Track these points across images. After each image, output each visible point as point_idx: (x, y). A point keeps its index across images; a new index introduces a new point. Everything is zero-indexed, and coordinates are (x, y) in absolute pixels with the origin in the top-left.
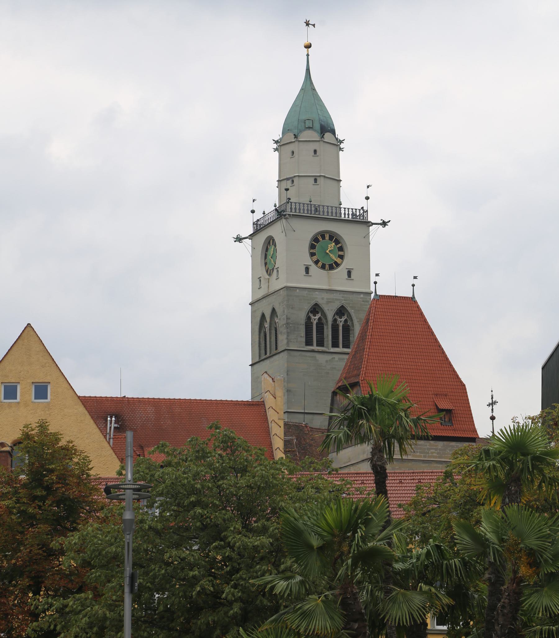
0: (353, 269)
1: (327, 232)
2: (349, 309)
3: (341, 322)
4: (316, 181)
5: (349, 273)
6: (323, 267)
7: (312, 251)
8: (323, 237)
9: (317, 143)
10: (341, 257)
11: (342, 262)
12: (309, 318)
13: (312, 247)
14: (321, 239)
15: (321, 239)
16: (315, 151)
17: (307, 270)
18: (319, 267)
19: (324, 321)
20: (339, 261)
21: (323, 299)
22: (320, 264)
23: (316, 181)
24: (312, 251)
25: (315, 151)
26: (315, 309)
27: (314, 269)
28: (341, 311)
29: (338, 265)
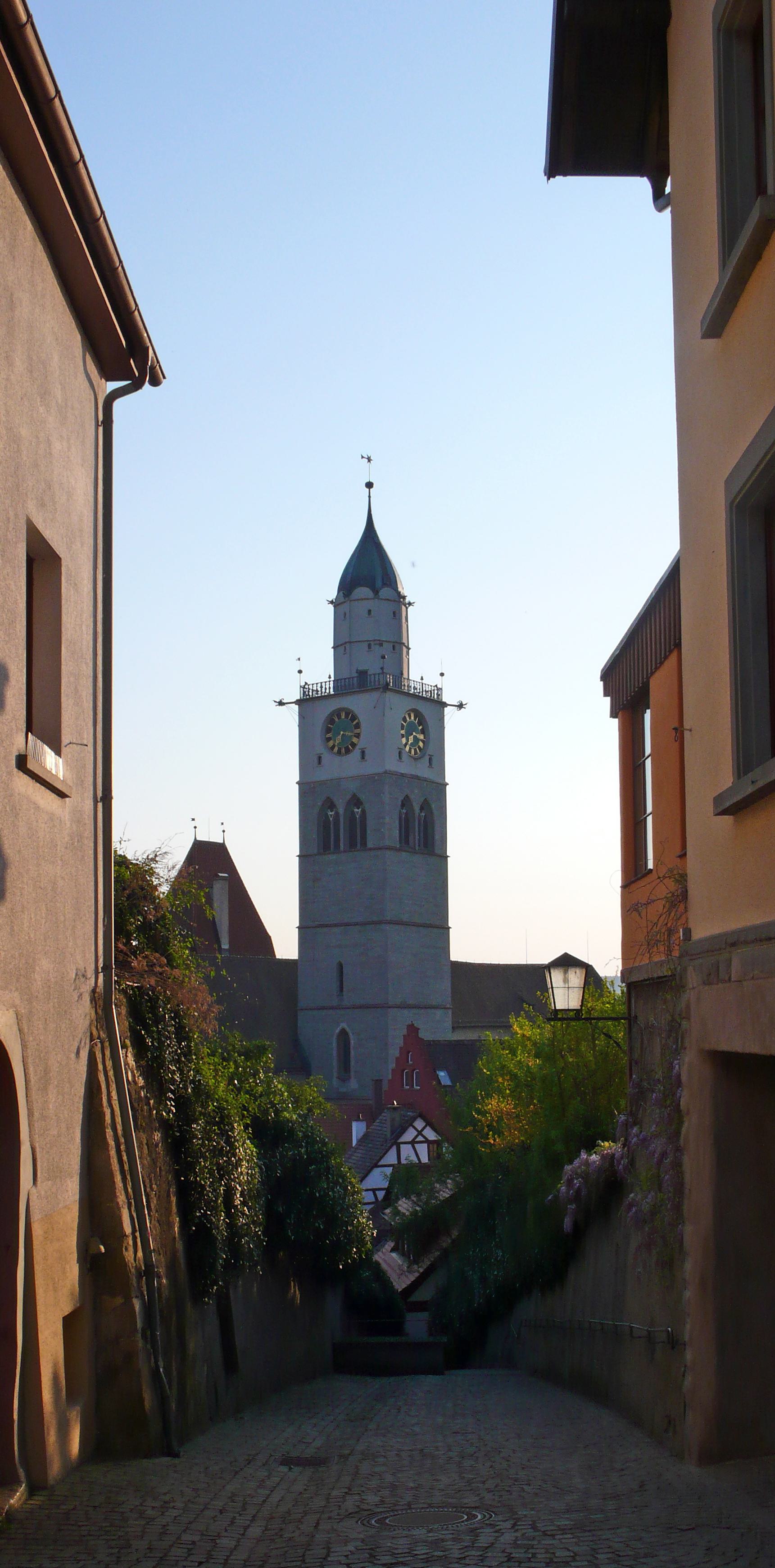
0: (365, 748)
5: (363, 753)
8: (339, 717)
10: (358, 736)
11: (358, 742)
13: (328, 730)
14: (337, 720)
15: (337, 720)
17: (320, 758)
18: (334, 753)
20: (355, 740)
24: (327, 736)
27: (327, 757)
28: (356, 801)
29: (354, 745)
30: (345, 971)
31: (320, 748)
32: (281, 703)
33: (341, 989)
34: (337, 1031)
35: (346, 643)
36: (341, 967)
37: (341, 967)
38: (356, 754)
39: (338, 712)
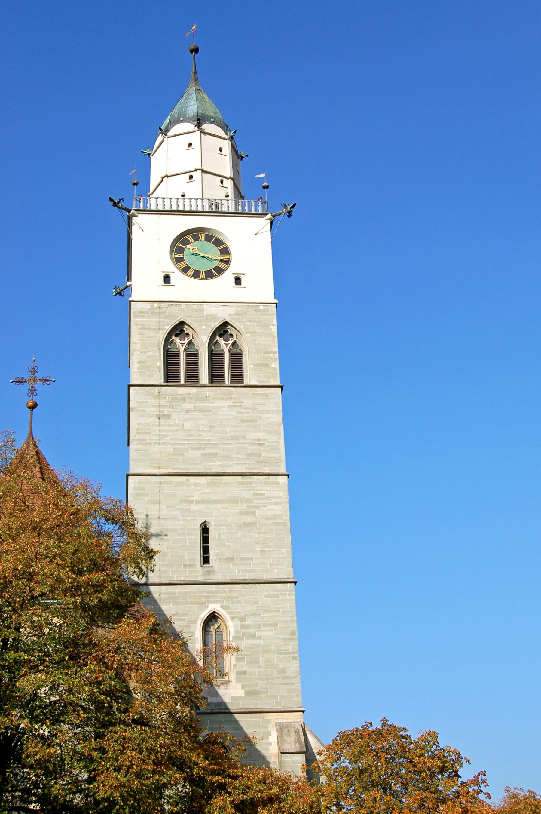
1: (201, 230)
4: (191, 177)
5: (238, 281)
7: (177, 256)
11: (227, 268)
17: (167, 279)
22: (191, 272)
23: (191, 177)
24: (177, 256)
30: (212, 534)
31: (169, 266)
32: (115, 205)
33: (206, 560)
34: (204, 614)
35: (196, 170)
36: (205, 530)
37: (205, 530)
38: (228, 277)
39: (195, 233)
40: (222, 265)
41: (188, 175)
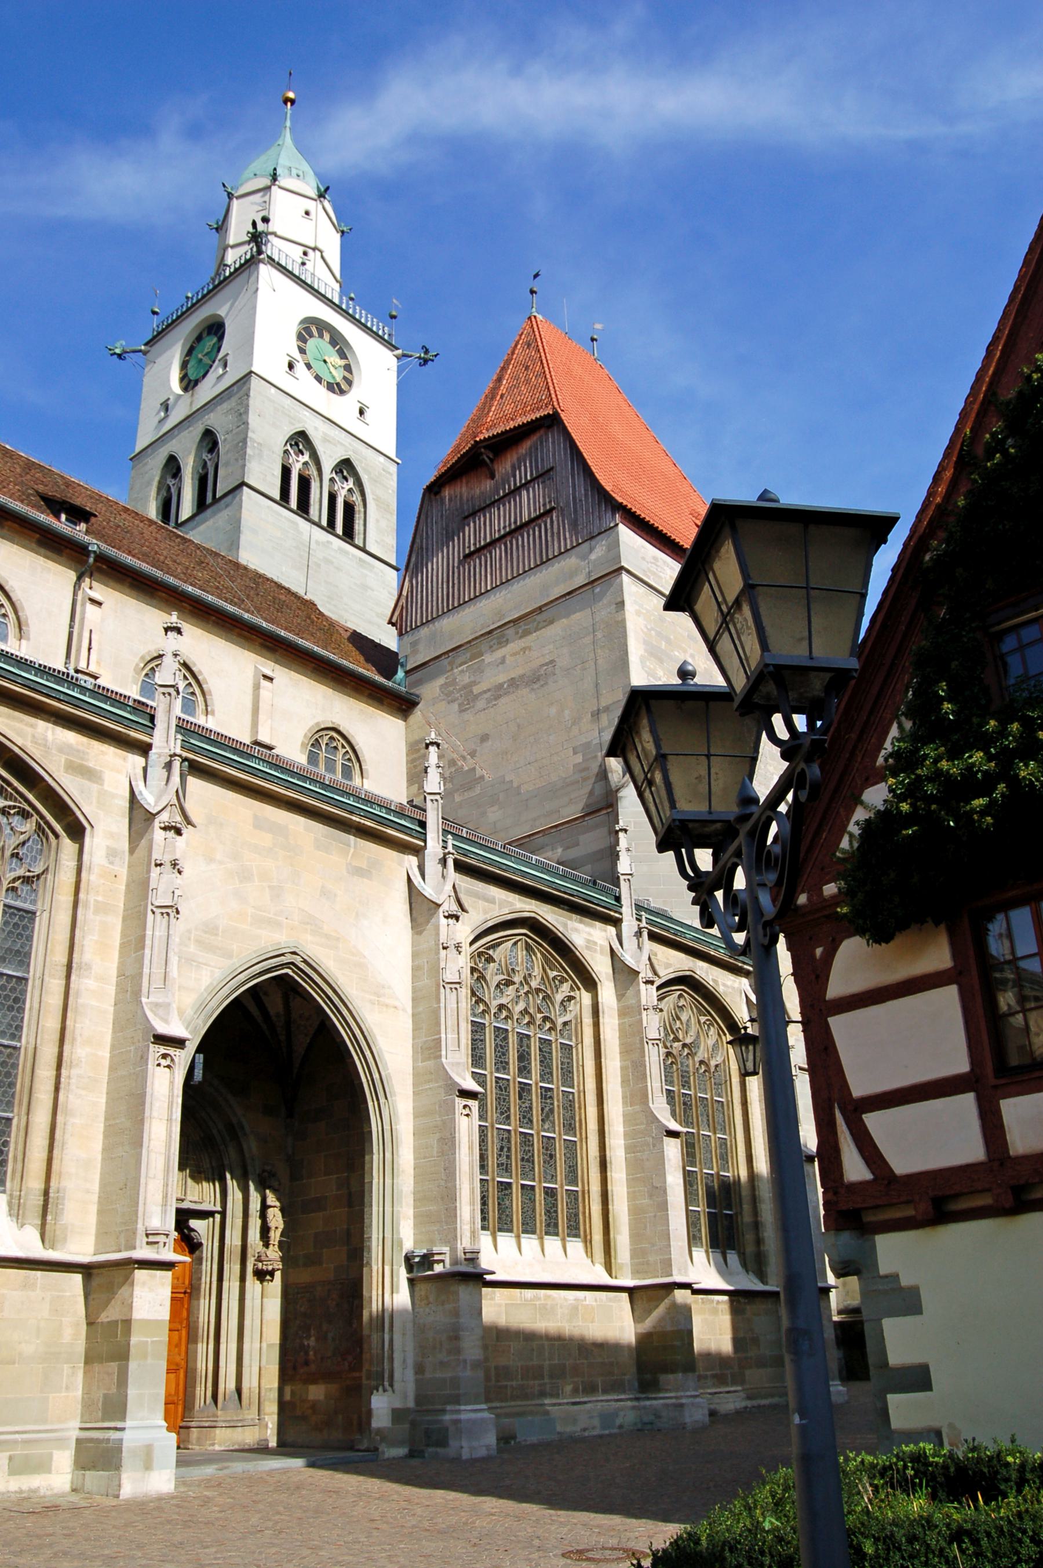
2: (359, 469)
3: (343, 489)
6: (318, 379)
9: (314, 202)
12: (286, 452)
15: (315, 333)
16: (307, 213)
19: (313, 471)
21: (316, 429)
23: (305, 254)
25: (307, 213)
26: (301, 440)
28: (345, 467)
35: (314, 249)
39: (321, 326)
40: (344, 386)
41: (301, 249)
